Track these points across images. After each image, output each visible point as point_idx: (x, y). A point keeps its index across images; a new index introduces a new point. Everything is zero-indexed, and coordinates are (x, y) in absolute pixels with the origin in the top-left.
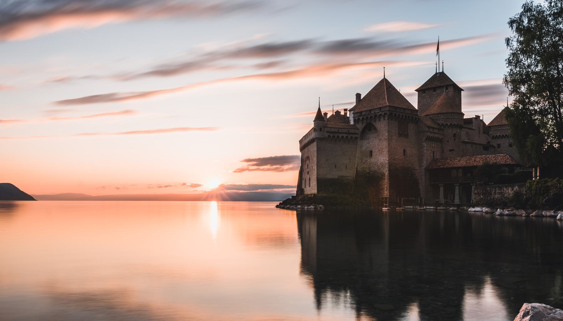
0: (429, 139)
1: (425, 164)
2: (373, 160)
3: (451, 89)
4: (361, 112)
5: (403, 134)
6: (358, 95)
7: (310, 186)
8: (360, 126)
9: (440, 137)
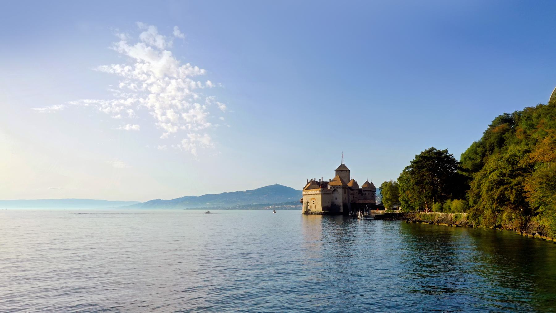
0: (351, 194)
1: (350, 202)
2: (337, 201)
3: (348, 172)
4: (333, 186)
5: (345, 193)
6: (330, 179)
7: (315, 208)
8: (332, 190)
9: (353, 193)
